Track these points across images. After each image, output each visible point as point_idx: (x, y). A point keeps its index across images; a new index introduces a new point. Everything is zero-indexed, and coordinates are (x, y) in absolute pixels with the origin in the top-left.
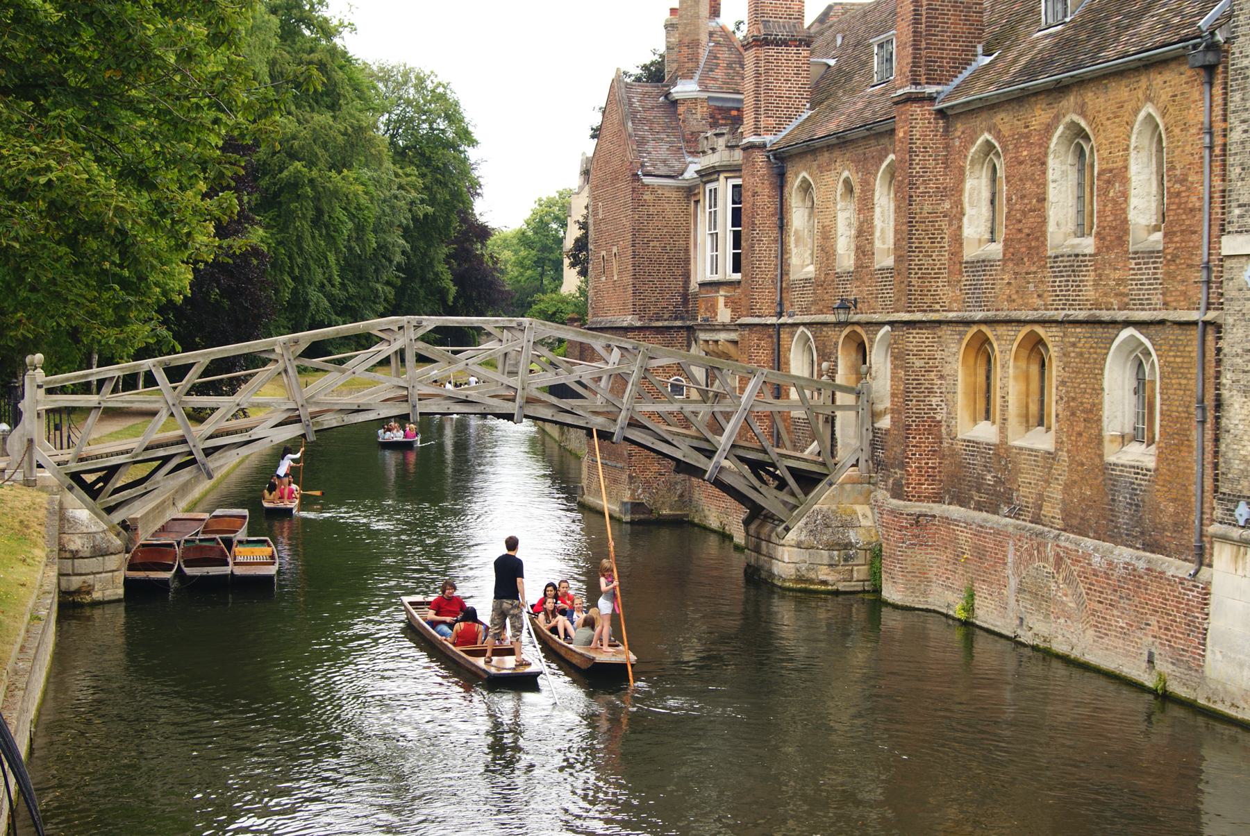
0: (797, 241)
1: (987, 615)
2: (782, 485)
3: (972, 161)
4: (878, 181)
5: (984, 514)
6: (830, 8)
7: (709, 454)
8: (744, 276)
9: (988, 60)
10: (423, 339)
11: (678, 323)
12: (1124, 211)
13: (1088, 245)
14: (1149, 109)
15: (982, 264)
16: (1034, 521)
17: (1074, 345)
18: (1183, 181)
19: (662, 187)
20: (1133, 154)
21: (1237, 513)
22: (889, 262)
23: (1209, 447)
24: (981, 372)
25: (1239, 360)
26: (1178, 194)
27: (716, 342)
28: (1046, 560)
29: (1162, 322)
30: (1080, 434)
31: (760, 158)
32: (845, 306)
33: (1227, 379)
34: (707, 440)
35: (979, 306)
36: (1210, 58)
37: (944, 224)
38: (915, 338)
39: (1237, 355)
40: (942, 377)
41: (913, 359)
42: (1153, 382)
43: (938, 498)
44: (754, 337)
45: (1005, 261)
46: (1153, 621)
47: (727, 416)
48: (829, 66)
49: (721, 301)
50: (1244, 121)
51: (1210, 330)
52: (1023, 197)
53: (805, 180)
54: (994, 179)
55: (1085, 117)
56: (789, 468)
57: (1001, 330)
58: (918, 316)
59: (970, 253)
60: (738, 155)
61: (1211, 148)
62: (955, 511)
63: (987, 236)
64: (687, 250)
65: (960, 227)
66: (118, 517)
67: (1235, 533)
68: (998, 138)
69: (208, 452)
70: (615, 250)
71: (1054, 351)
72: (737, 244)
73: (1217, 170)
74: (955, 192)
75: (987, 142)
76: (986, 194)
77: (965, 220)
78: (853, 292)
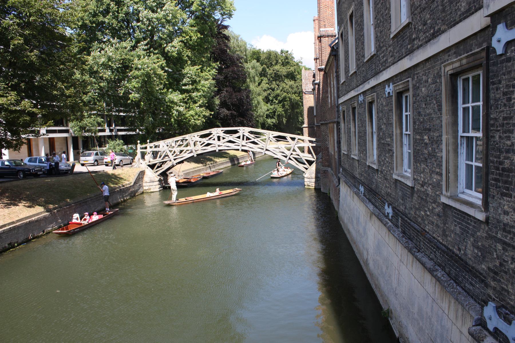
7: (286, 157)
34: (284, 153)
41: (323, 133)
43: (329, 166)
49: (315, 120)
56: (306, 160)
58: (323, 122)
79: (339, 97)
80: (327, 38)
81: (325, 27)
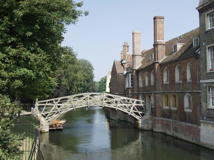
0: (140, 82)
1: (168, 133)
2: (139, 115)
3: (165, 71)
4: (151, 74)
5: (167, 119)
6: (143, 51)
7: (129, 111)
8: (133, 87)
9: (166, 57)
10: (90, 96)
11: (123, 94)
12: (186, 77)
13: (181, 82)
14: (189, 63)
15: (166, 85)
16: (175, 120)
17: (180, 95)
18: (194, 73)
19: (121, 75)
20: (187, 69)
21: (204, 118)
22: (153, 85)
23: (199, 109)
24: (167, 100)
25: (203, 97)
26: (194, 75)
27: (129, 96)
28: (177, 125)
29: (192, 92)
30: (181, 108)
31: (135, 71)
32: (147, 91)
33: (202, 100)
35: (166, 90)
36: (198, 56)
37: (161, 80)
38: (157, 95)
39: (203, 96)
40: (161, 100)
41: (157, 98)
42: (191, 100)
44: (134, 95)
45: (169, 84)
46: (192, 133)
47: (131, 106)
48: (143, 58)
49: (130, 90)
50: (203, 65)
51: (199, 93)
52: (172, 75)
53: (141, 74)
54: (167, 73)
55: (180, 65)
57: (169, 94)
58: (157, 92)
59: (164, 83)
60: (132, 71)
61: (198, 68)
62: (164, 119)
63: (167, 81)
64: (125, 84)
65: (163, 80)
66: (48, 120)
67: (204, 121)
68: (168, 68)
69: (60, 112)
70: (115, 84)
71: (177, 96)
72: (132, 82)
73: (199, 71)
74: (162, 75)
75: (166, 68)
76: (166, 75)
77: (164, 79)
78: (148, 89)
79: (200, 79)
80: (161, 46)
81: (159, 40)
